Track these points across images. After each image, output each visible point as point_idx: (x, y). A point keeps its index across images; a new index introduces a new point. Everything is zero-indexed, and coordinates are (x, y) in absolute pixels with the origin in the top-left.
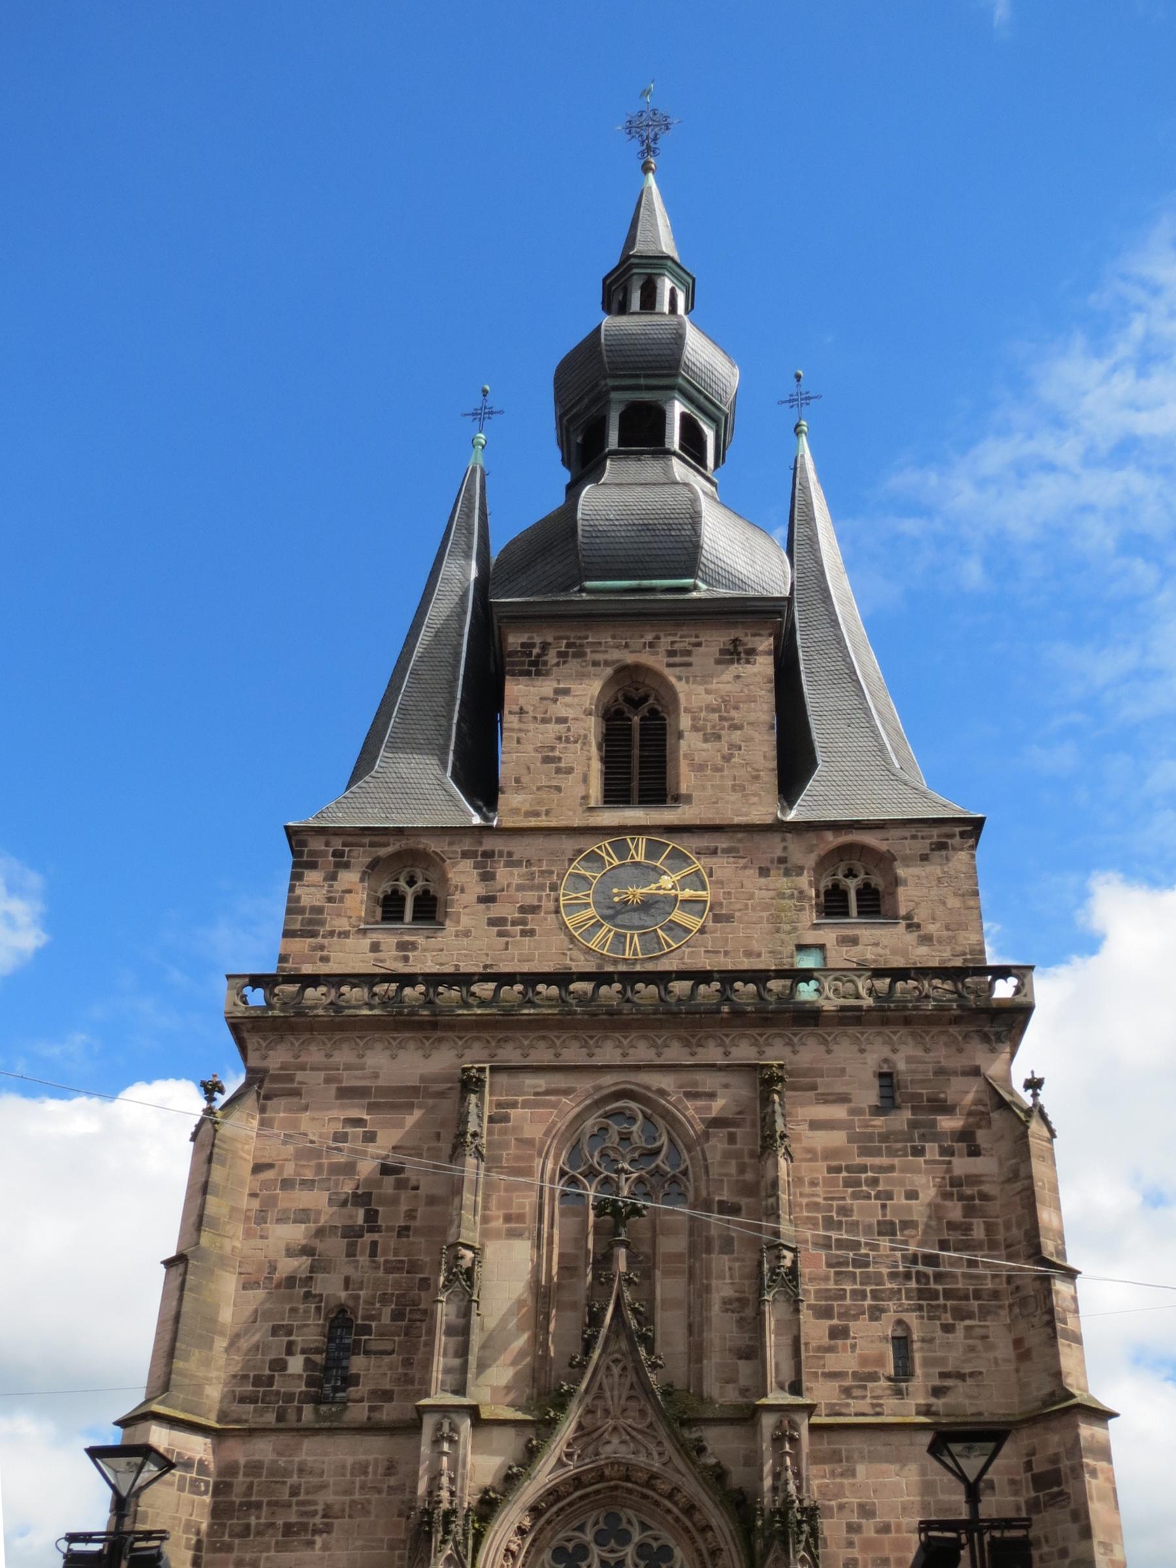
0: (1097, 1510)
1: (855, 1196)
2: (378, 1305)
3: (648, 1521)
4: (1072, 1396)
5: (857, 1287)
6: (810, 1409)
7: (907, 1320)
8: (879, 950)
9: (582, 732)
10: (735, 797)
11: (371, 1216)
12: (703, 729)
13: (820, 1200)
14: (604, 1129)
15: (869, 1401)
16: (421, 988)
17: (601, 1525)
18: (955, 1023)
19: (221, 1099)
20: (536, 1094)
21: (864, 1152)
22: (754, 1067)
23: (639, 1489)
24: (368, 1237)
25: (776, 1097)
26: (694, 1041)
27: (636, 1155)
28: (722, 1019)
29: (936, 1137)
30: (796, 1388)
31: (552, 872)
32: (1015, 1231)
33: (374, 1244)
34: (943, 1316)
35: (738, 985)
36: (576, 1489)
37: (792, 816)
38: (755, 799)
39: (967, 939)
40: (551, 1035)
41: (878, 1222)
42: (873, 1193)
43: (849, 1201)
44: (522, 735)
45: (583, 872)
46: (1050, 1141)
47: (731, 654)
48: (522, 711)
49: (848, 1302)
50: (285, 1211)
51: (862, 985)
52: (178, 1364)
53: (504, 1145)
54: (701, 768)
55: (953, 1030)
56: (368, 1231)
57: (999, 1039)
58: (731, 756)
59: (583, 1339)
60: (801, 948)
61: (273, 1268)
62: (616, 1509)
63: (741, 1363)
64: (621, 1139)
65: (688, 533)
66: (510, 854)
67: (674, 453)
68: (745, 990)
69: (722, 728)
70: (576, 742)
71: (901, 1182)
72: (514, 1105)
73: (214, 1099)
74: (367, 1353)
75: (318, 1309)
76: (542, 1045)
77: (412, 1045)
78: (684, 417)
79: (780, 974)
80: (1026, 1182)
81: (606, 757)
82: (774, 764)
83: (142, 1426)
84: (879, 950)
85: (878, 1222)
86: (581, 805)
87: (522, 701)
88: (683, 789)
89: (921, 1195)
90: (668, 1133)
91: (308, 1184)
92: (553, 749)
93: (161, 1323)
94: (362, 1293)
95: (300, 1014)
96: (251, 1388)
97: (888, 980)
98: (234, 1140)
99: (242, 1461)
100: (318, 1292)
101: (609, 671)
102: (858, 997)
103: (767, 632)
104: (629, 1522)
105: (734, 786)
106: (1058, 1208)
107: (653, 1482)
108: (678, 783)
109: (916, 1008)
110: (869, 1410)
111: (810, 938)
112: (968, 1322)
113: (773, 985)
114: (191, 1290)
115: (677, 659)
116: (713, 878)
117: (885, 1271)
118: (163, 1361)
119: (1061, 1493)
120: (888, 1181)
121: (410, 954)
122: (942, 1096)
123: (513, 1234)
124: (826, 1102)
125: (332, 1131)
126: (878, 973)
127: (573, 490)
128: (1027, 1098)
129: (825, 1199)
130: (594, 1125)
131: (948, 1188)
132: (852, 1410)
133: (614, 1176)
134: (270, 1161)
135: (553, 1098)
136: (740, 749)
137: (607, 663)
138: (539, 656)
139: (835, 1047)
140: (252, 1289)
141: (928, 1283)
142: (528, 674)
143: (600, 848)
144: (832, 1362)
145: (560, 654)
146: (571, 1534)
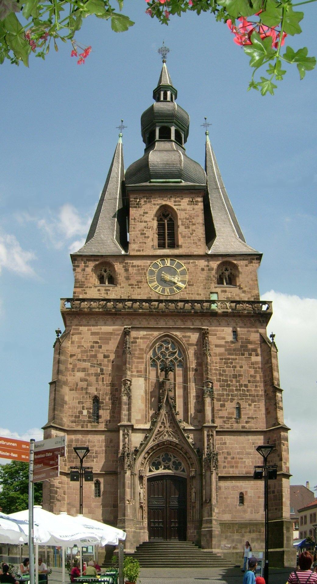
0: (284, 453)
1: (227, 367)
2: (105, 396)
3: (175, 456)
4: (280, 424)
5: (228, 393)
6: (216, 427)
7: (239, 402)
8: (232, 294)
9: (151, 226)
10: (194, 246)
11: (102, 370)
12: (185, 224)
13: (218, 368)
14: (162, 346)
15: (230, 424)
16: (112, 303)
17: (164, 456)
18: (252, 317)
19: (60, 335)
20: (143, 335)
21: (229, 354)
22: (200, 329)
23: (173, 447)
24: (101, 376)
25: (207, 338)
26: (184, 320)
27: (170, 354)
28: (192, 314)
29: (247, 350)
30: (213, 421)
31: (144, 269)
32: (267, 378)
33: (103, 378)
34: (249, 402)
35: (196, 304)
36: (158, 447)
37: (210, 252)
38: (200, 247)
39: (255, 292)
40: (147, 317)
41: (233, 374)
42: (231, 366)
43: (225, 368)
44: (134, 226)
45: (153, 269)
46: (276, 353)
47: (191, 202)
48: (135, 219)
49: (225, 397)
50: (79, 368)
51: (228, 304)
52: (56, 412)
53: (136, 350)
54: (184, 237)
55: (252, 319)
56: (101, 375)
57: (263, 322)
58: (193, 233)
59: (159, 407)
60: (211, 293)
61: (77, 385)
62: (167, 452)
63: (198, 413)
64: (166, 349)
65: (179, 166)
66: (133, 263)
67: (174, 141)
68: (198, 306)
69: (190, 225)
70: (150, 229)
71: (238, 363)
72: (138, 338)
73: (59, 335)
74: (103, 409)
75: (90, 397)
76: (144, 320)
77: (110, 320)
78: (175, 130)
79: (207, 301)
80: (270, 364)
81: (158, 232)
82: (204, 236)
83: (49, 429)
84: (232, 294)
85: (233, 374)
86: (152, 248)
87: (134, 215)
88: (180, 244)
89: (243, 367)
90: (178, 347)
91: (84, 361)
92: (143, 231)
93: (50, 400)
94: (100, 392)
95: (81, 310)
96: (74, 419)
97: (235, 304)
98: (65, 348)
99: (74, 439)
100: (89, 392)
101: (158, 207)
102: (227, 309)
103: (200, 196)
104: (171, 456)
105: (194, 242)
106: (278, 372)
107: (177, 446)
108: (178, 241)
109: (242, 313)
110: (230, 427)
111: (214, 290)
112: (255, 403)
113: (205, 304)
114: (57, 391)
115: (177, 204)
116: (189, 271)
117: (234, 388)
118: (52, 411)
119: (276, 449)
120: (235, 363)
121: (108, 292)
122: (249, 338)
123: (139, 376)
124: (219, 339)
125: (90, 345)
126: (232, 302)
127: (147, 150)
128: (271, 339)
129: (219, 367)
130: (158, 345)
131: (250, 365)
132: (226, 427)
133: (164, 360)
134: (74, 354)
135: (148, 337)
136: (195, 231)
137: (158, 204)
138: (139, 202)
139: (221, 323)
140: (72, 391)
141: (245, 392)
142: (136, 207)
143: (157, 262)
144: (221, 414)
145: (145, 201)
146: (157, 459)
